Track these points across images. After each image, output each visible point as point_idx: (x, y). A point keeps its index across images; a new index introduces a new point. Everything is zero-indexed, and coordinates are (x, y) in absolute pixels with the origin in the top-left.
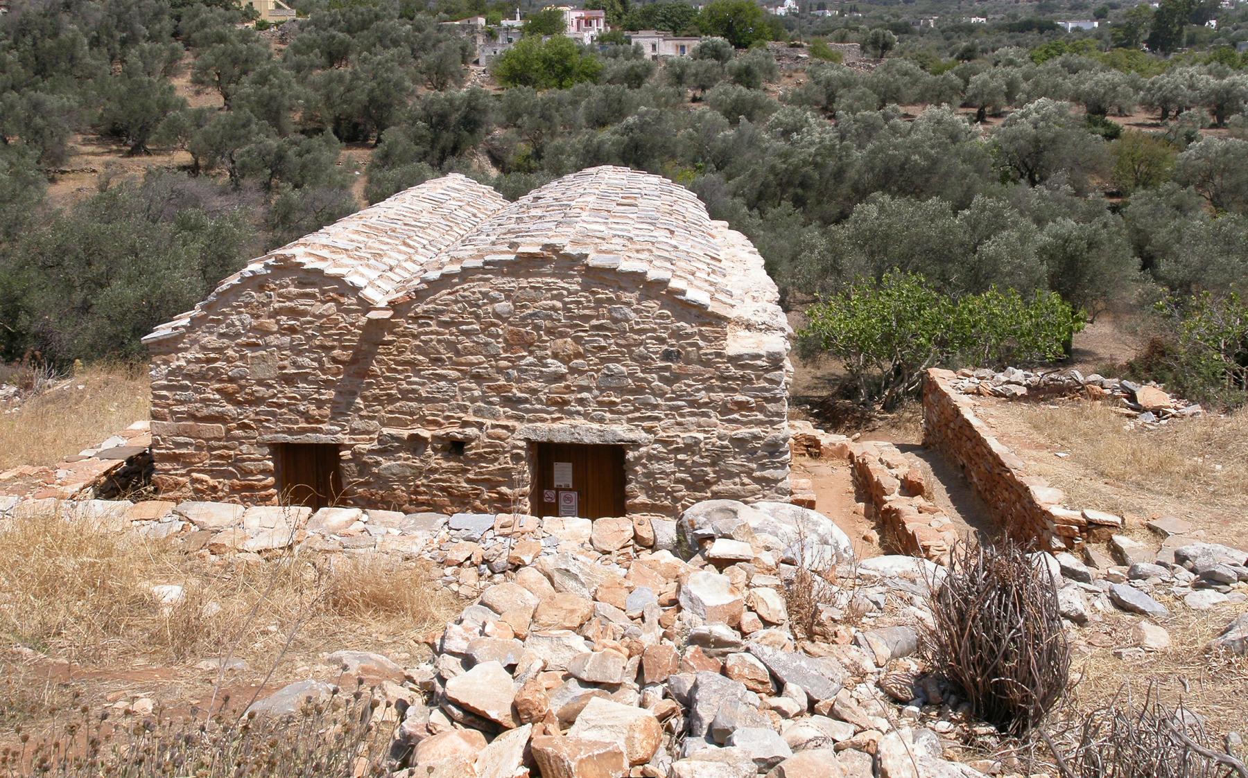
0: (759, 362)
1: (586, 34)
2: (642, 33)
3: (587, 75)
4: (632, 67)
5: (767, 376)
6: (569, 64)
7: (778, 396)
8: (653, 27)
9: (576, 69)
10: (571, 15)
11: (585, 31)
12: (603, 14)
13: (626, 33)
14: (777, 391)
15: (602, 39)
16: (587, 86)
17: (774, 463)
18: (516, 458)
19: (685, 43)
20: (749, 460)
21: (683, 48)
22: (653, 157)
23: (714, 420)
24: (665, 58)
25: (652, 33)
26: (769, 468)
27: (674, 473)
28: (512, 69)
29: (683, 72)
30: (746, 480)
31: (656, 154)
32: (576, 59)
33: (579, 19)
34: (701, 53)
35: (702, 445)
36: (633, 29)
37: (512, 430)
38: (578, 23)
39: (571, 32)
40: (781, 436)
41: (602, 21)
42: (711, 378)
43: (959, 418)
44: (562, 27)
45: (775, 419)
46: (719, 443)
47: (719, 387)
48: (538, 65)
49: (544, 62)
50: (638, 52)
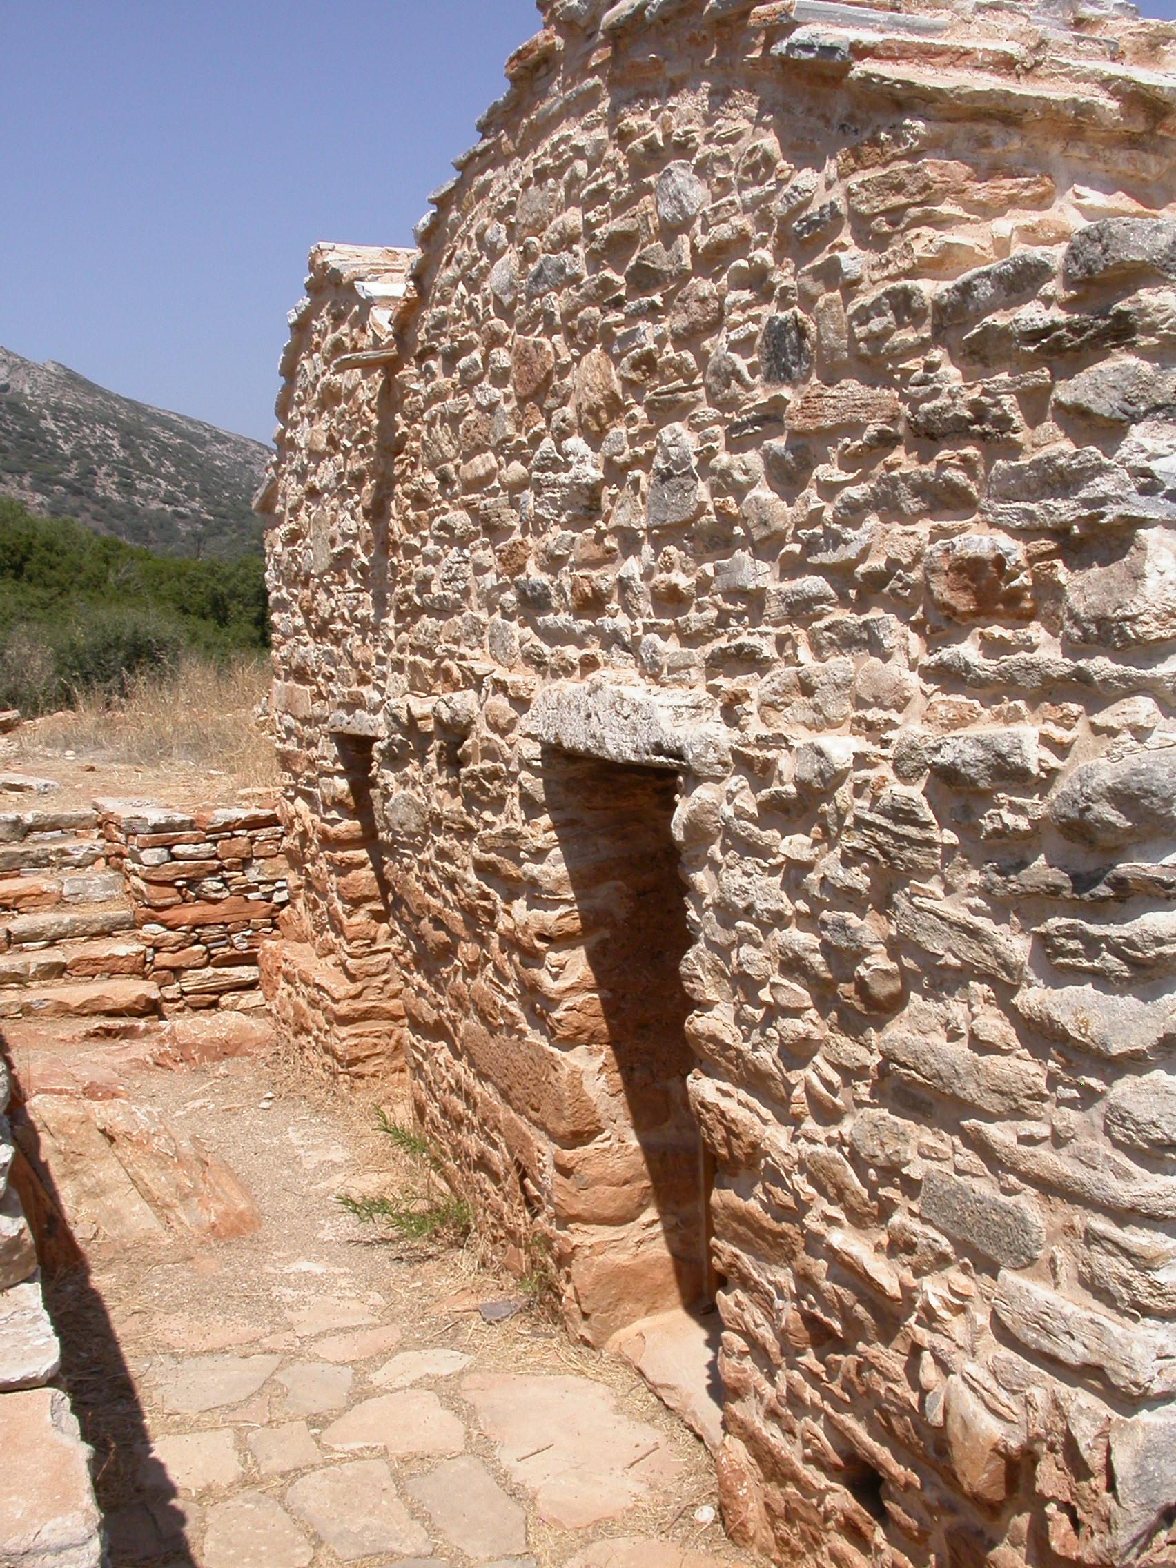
0: (1032, 314)
5: (1065, 392)
7: (1111, 513)
14: (1102, 485)
17: (1092, 945)
18: (530, 806)
20: (1000, 909)
23: (897, 669)
26: (1078, 975)
27: (779, 920)
30: (993, 1025)
35: (844, 793)
37: (521, 704)
40: (1107, 773)
42: (886, 441)
45: (1101, 665)
46: (897, 790)
47: (921, 489)
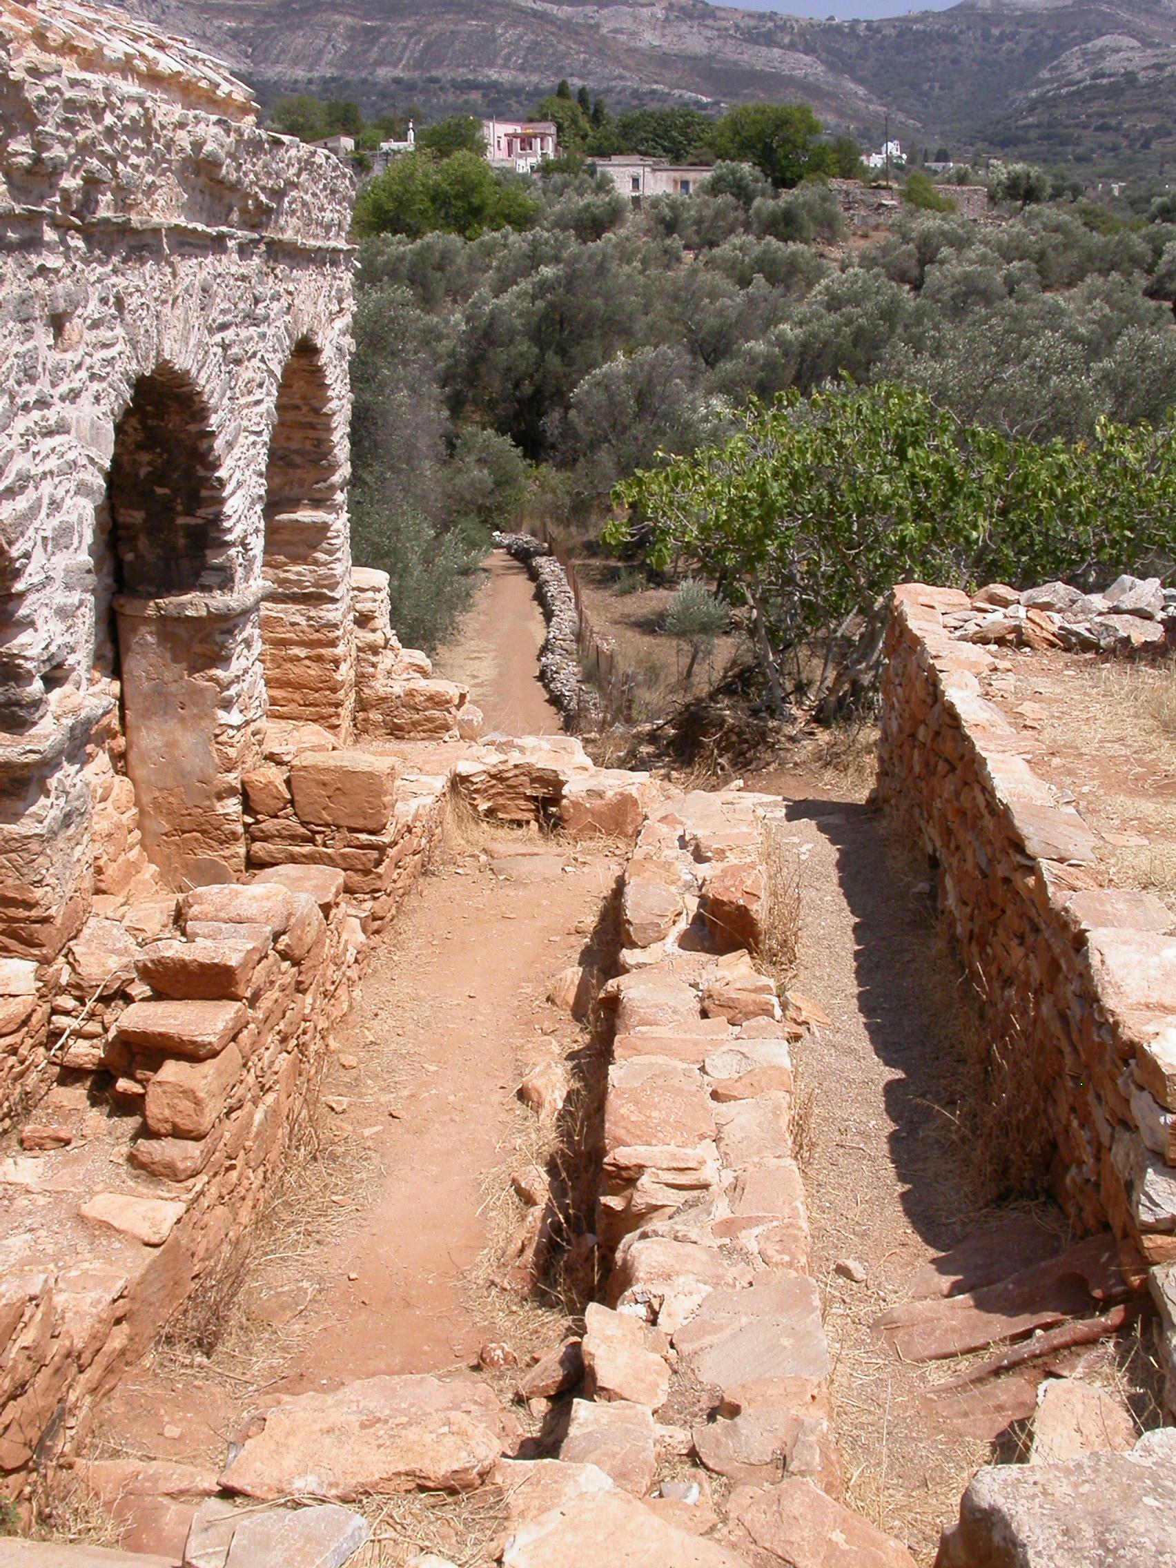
1: (521, 162)
2: (616, 159)
3: (508, 219)
4: (587, 207)
6: (476, 201)
8: (633, 151)
9: (489, 211)
10: (497, 132)
11: (521, 156)
12: (553, 130)
13: (589, 160)
15: (545, 169)
16: (505, 237)
19: (690, 176)
21: (685, 184)
22: (591, 337)
24: (655, 203)
25: (635, 159)
28: (378, 209)
29: (676, 218)
31: (598, 332)
32: (489, 195)
33: (511, 137)
34: (714, 188)
36: (603, 153)
38: (510, 144)
39: (496, 156)
41: (550, 142)
43: (938, 707)
44: (482, 148)
48: (423, 204)
49: (433, 199)
50: (604, 185)
